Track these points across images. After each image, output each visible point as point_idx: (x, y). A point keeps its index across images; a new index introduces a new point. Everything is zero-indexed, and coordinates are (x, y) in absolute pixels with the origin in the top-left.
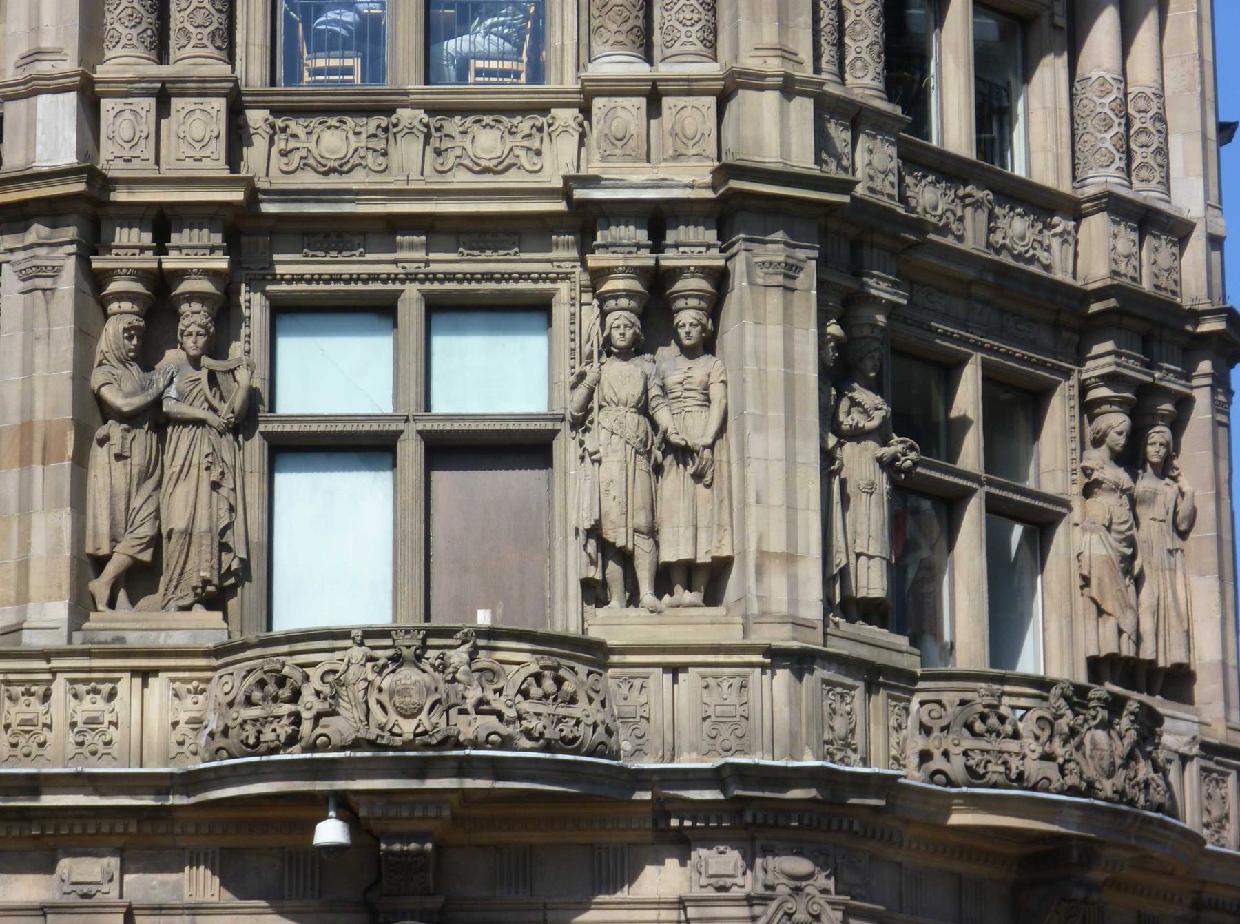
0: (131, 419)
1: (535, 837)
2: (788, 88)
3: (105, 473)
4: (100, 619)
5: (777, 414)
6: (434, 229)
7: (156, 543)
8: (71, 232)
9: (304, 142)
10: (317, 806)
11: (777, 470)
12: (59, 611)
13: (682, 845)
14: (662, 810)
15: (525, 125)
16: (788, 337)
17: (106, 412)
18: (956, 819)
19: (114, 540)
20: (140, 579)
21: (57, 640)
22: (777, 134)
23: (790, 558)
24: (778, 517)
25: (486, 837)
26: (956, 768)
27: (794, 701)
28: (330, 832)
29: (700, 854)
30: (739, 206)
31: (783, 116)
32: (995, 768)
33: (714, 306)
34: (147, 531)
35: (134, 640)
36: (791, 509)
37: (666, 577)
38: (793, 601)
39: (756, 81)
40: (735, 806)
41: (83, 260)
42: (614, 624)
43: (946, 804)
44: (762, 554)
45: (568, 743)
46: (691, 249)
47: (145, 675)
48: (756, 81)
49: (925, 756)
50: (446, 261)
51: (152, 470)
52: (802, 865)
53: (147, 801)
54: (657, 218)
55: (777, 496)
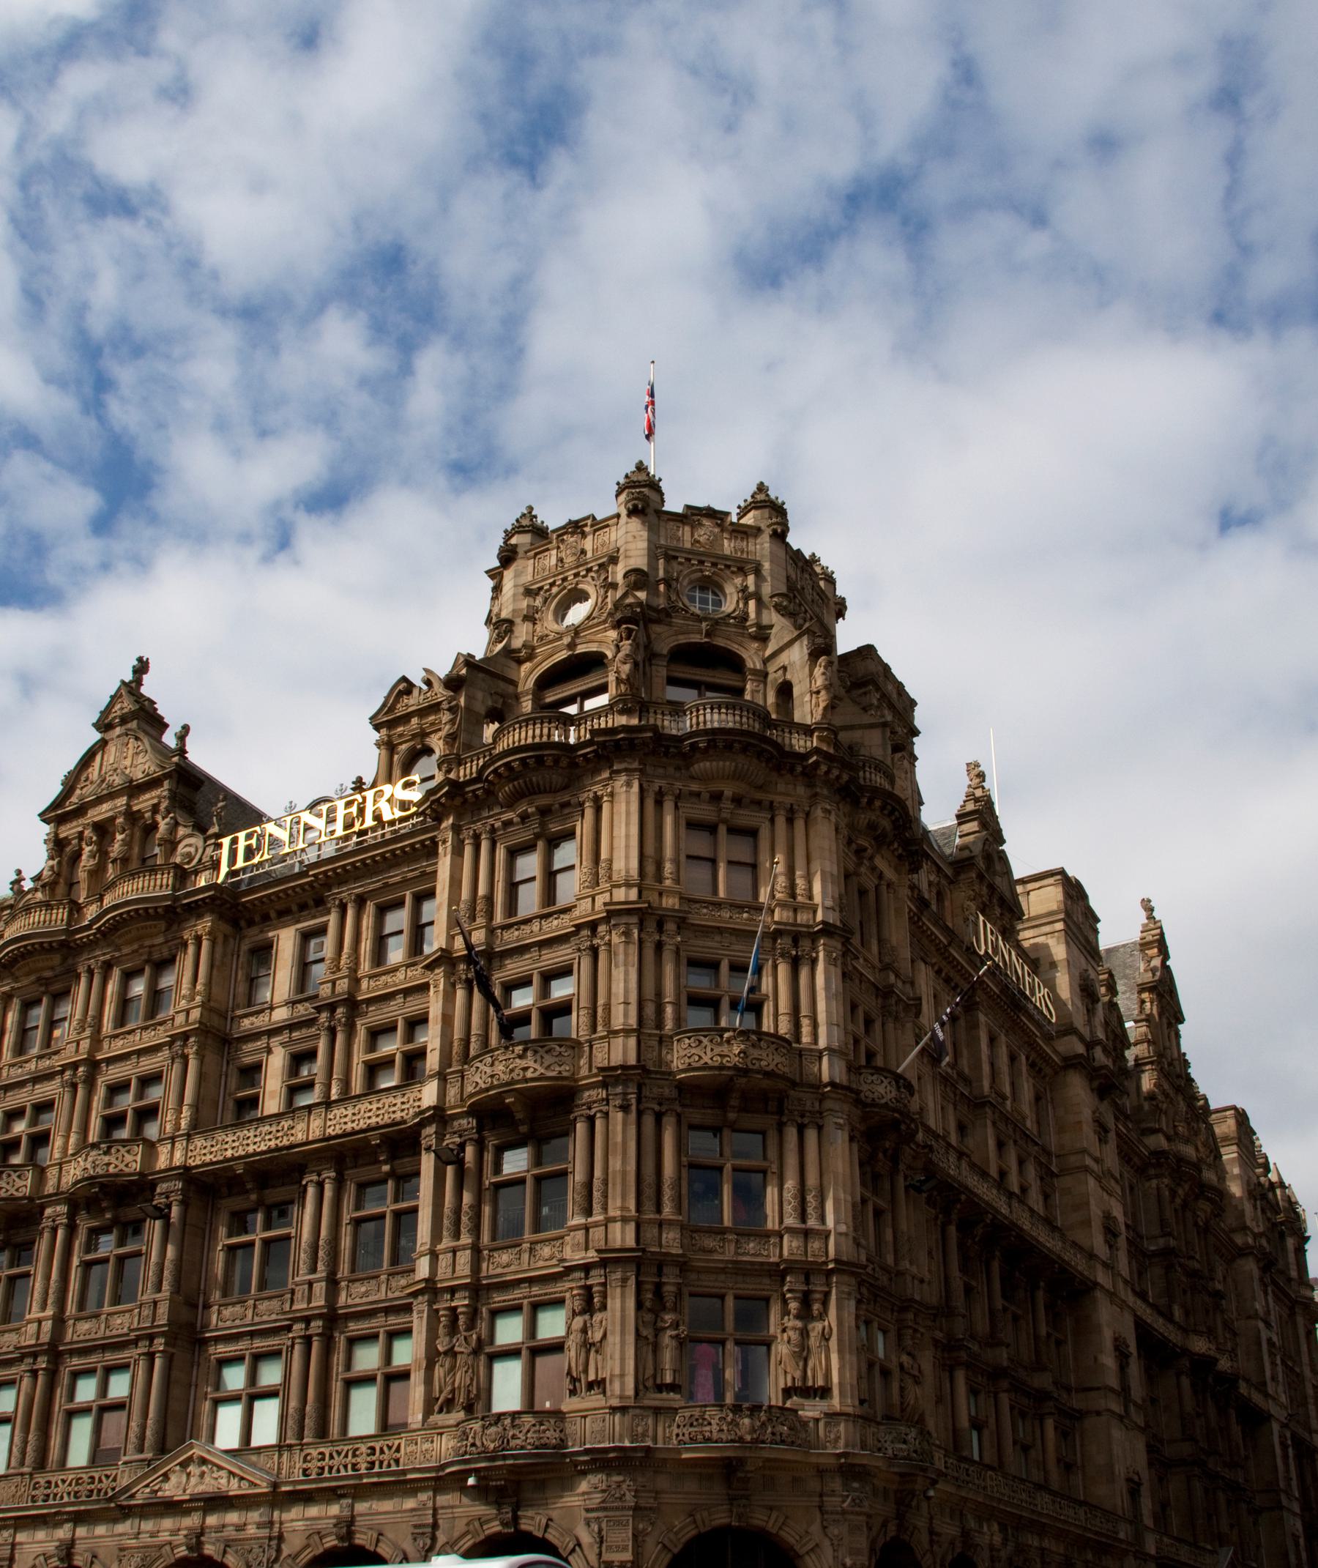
0: (446, 1353)
1: (543, 1476)
2: (624, 1220)
3: (439, 1372)
4: (432, 1418)
5: (618, 1328)
6: (531, 1281)
7: (453, 1391)
8: (426, 1297)
9: (497, 1259)
10: (468, 1473)
11: (618, 1347)
12: (420, 1417)
13: (584, 1473)
14: (576, 1464)
15: (558, 1243)
16: (623, 1302)
17: (439, 1353)
18: (684, 1456)
19: (441, 1392)
20: (448, 1405)
21: (419, 1426)
22: (622, 1236)
23: (622, 1375)
24: (618, 1362)
25: (533, 1477)
26: (686, 1438)
27: (622, 1423)
28: (471, 1481)
29: (590, 1477)
30: (608, 1260)
31: (623, 1232)
32: (700, 1437)
33: (604, 1295)
34: (449, 1388)
35: (440, 1423)
36: (623, 1359)
37: (590, 1386)
38: (622, 1389)
39: (614, 1220)
40: (593, 1461)
41: (430, 1306)
42: (569, 1404)
43: (679, 1451)
44: (612, 1376)
45: (545, 1446)
46: (595, 1279)
47: (441, 1434)
48: (614, 1220)
49: (678, 1435)
50: (536, 1290)
51: (453, 1368)
52: (620, 1478)
53: (433, 1475)
54: (587, 1268)
55: (617, 1356)
